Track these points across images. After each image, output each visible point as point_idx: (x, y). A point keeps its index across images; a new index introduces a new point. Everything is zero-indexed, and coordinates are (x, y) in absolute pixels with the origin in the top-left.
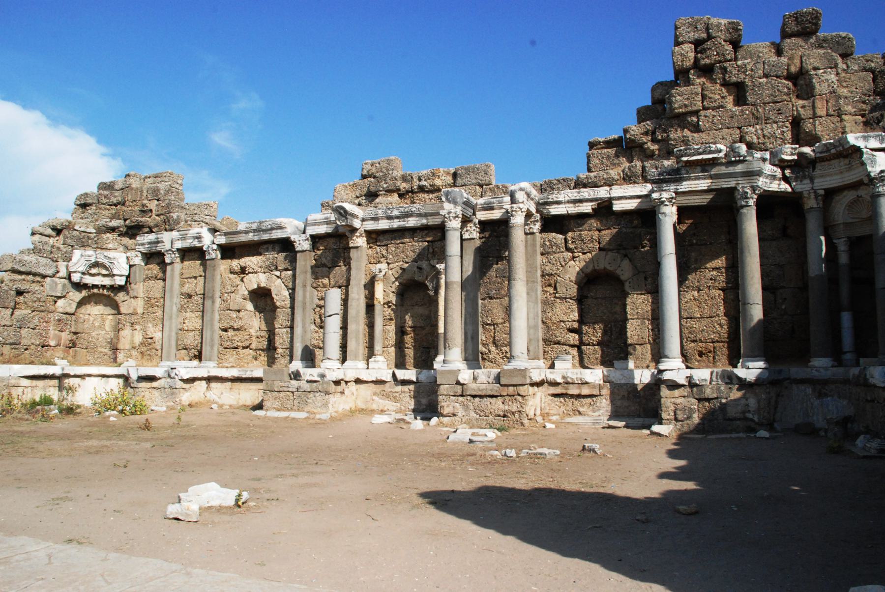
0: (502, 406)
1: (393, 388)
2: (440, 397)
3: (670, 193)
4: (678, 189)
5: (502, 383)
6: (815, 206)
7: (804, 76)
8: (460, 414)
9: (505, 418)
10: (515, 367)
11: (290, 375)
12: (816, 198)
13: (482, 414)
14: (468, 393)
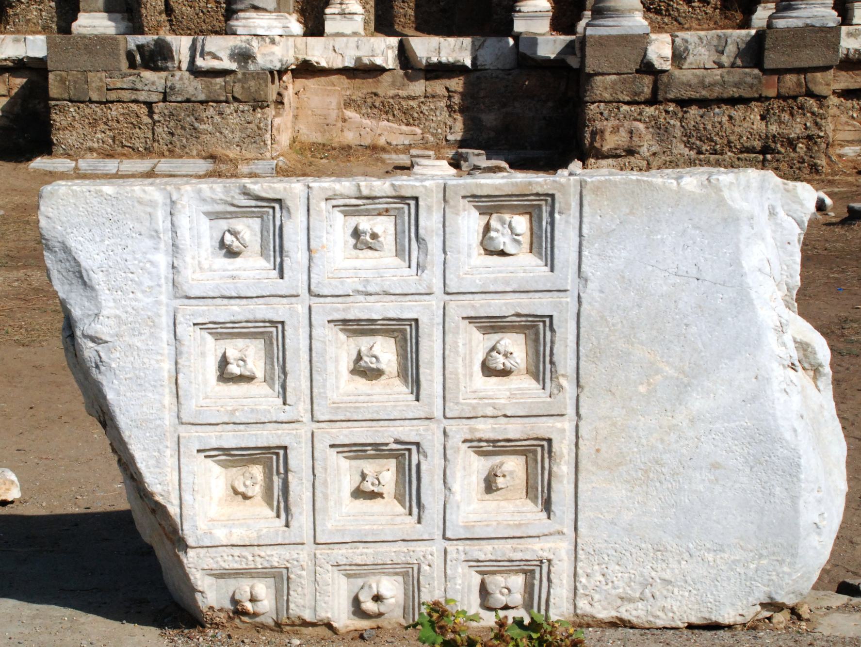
0: (759, 126)
1: (403, 86)
2: (592, 107)
5: (768, 64)
8: (644, 151)
9: (769, 157)
10: (809, 21)
11: (130, 56)
13: (705, 147)
14: (671, 96)
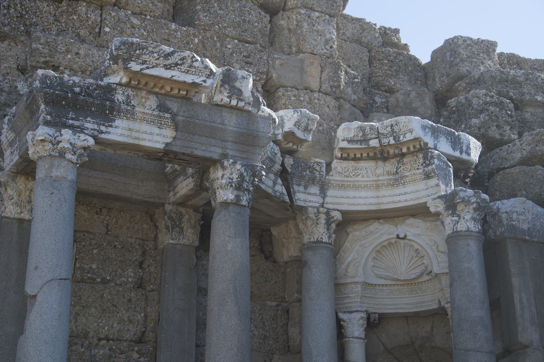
3: (83, 136)
4: (102, 132)
6: (325, 239)
7: (288, 13)
12: (328, 223)
